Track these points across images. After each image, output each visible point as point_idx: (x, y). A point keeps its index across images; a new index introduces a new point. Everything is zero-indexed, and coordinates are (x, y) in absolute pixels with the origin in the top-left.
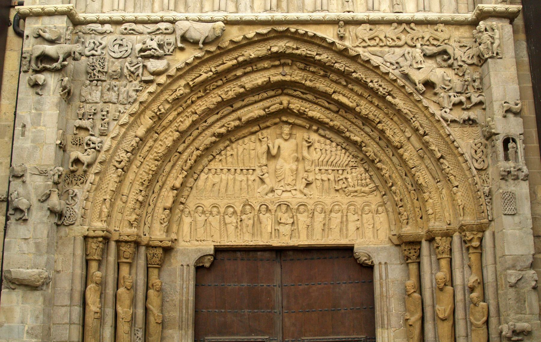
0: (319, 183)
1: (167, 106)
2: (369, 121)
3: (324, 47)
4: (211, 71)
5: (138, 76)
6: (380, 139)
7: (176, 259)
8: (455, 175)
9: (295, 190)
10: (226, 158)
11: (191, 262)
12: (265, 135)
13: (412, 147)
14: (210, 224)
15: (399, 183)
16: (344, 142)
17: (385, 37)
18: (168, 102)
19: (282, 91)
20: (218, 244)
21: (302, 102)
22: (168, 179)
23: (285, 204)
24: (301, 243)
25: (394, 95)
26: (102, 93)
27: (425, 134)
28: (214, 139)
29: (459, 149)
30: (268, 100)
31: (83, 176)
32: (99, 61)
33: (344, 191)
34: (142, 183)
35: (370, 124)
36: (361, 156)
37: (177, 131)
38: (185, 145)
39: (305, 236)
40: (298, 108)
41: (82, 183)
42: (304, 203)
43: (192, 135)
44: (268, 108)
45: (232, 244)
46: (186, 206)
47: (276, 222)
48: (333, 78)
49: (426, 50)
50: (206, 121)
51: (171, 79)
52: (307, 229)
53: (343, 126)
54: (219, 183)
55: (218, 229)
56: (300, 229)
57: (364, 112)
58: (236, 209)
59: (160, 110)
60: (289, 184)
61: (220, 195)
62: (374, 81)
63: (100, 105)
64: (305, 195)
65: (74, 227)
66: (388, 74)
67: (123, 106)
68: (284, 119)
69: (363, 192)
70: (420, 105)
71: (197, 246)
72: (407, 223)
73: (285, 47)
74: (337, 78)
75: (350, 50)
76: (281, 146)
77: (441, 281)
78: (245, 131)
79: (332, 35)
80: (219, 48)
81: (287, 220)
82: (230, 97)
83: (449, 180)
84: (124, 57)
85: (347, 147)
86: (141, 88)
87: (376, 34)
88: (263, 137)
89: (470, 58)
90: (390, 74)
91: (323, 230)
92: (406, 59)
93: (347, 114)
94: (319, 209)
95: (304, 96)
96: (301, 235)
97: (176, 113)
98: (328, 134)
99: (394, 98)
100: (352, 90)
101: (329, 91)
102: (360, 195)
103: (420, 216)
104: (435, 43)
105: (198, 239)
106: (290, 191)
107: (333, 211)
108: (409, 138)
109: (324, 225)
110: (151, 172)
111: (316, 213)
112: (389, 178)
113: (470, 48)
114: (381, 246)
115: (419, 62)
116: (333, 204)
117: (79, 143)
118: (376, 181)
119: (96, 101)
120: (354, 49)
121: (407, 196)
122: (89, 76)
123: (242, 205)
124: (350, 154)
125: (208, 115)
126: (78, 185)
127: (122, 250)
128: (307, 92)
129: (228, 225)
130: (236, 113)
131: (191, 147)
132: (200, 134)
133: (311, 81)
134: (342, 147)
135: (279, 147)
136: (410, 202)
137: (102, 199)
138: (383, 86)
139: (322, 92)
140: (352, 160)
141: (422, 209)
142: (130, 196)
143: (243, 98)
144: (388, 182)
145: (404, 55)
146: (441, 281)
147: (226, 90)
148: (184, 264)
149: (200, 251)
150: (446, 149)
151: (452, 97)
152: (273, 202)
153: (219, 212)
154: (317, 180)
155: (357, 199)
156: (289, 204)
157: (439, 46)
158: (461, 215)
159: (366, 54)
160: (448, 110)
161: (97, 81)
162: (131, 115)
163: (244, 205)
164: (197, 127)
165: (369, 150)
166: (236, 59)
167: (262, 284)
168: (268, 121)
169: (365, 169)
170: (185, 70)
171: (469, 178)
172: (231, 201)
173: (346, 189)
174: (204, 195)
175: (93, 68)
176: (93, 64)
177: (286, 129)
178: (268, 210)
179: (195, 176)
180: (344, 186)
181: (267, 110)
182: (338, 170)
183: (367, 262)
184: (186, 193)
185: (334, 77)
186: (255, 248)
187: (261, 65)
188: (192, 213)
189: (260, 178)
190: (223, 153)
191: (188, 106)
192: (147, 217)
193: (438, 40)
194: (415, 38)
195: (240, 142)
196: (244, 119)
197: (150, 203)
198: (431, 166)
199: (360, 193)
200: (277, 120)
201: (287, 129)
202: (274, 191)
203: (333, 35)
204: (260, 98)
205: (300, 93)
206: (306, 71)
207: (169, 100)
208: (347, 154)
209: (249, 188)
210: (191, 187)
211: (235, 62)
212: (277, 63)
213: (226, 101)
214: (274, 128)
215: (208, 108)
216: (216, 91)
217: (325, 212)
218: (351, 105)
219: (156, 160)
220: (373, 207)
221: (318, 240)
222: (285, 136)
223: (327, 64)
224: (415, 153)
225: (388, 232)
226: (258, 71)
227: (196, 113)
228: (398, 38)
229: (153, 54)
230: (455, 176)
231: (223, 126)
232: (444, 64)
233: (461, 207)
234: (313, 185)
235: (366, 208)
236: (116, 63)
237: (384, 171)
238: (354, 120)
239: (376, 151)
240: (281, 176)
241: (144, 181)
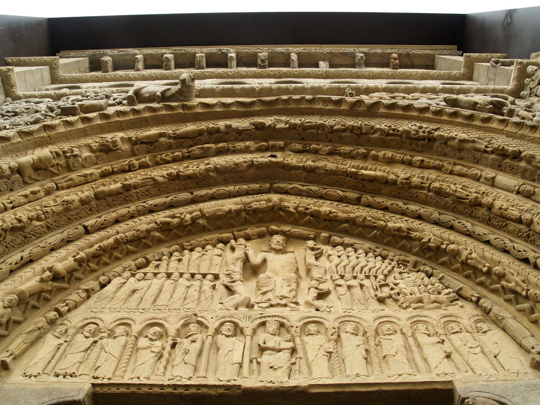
0: (342, 290)
1: (86, 154)
2: (414, 191)
6: (440, 214)
9: (297, 303)
10: (168, 265)
13: (504, 192)
16: (377, 248)
18: (92, 150)
19: (271, 184)
21: (302, 198)
22: (46, 258)
30: (250, 197)
33: (396, 301)
36: (412, 258)
40: (295, 205)
42: (315, 319)
44: (249, 203)
45: (138, 382)
46: (65, 322)
47: (256, 349)
48: (346, 149)
51: (104, 122)
52: (329, 360)
53: (372, 217)
54: (145, 289)
56: (310, 359)
57: (402, 176)
58: (166, 325)
59: (72, 151)
60: (283, 297)
64: (317, 310)
68: (274, 227)
74: (352, 149)
80: (184, 107)
81: (280, 344)
82: (191, 172)
91: (366, 359)
93: (375, 199)
94: (349, 327)
95: (305, 188)
96: (314, 368)
98: (347, 240)
100: (376, 158)
101: (342, 167)
105: (59, 372)
106: (285, 305)
107: (380, 333)
110: (15, 221)
111: (343, 335)
116: (378, 321)
123: (182, 322)
125: (152, 197)
129: (140, 351)
130: (198, 205)
133: (313, 161)
134: (374, 254)
135: (265, 261)
143: (210, 188)
144: (480, 266)
147: (185, 165)
154: (338, 288)
155: (425, 313)
156: (284, 321)
162: (21, 134)
163: (186, 325)
164: (128, 205)
165: (425, 234)
168: (247, 229)
169: (426, 273)
172: (161, 316)
174: (108, 306)
177: (278, 239)
178: (238, 330)
182: (376, 277)
184: (74, 297)
185: (347, 149)
187: (241, 145)
188: (71, 331)
195: (198, 249)
199: (429, 303)
200: (263, 229)
201: (278, 238)
202: (253, 306)
206: (305, 154)
208: (387, 261)
209: (203, 295)
210: (87, 291)
213: (183, 176)
214: (257, 243)
215: (153, 179)
216: (170, 165)
217: (365, 333)
221: (357, 375)
222: (276, 246)
223: (335, 128)
225: (522, 358)
226: (235, 152)
234: (332, 297)
237: (465, 253)
240: (267, 286)
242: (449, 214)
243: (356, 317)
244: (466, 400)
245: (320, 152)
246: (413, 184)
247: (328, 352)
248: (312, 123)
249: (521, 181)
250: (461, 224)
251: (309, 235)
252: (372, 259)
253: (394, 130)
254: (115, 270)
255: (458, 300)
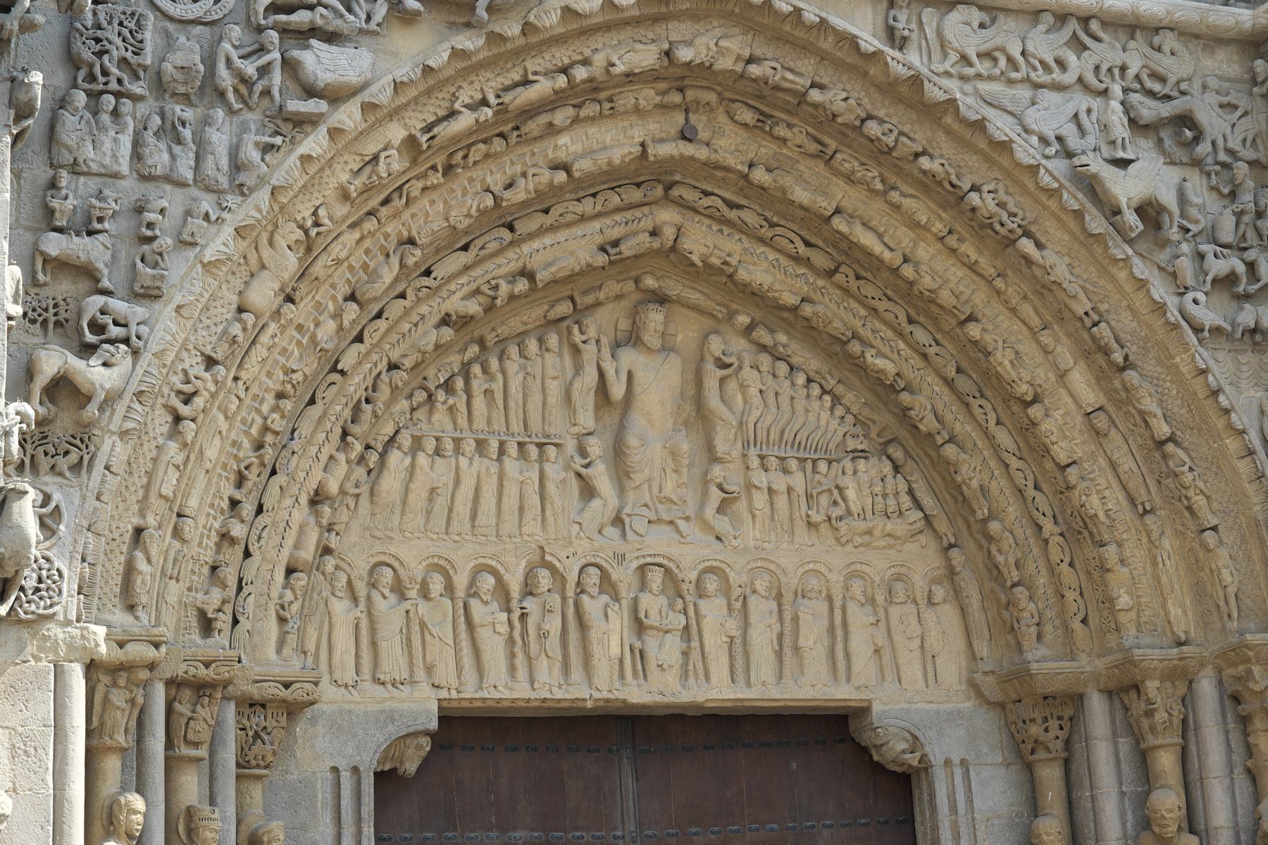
0: (760, 499)
1: (341, 210)
2: (934, 309)
3: (839, 64)
4: (484, 102)
5: (267, 93)
6: (959, 370)
7: (313, 746)
8: (1207, 493)
11: (366, 758)
12: (592, 332)
14: (423, 625)
15: (1010, 509)
17: (1023, 53)
20: (454, 695)
21: (721, 231)
23: (660, 565)
24: (714, 694)
25: (1038, 235)
26: (137, 143)
27: (1127, 365)
28: (447, 333)
29: (1233, 415)
31: (78, 442)
32: (121, 24)
34: (240, 472)
35: (935, 320)
37: (352, 297)
38: (362, 348)
39: (726, 673)
41: (76, 467)
43: (385, 316)
44: (616, 243)
45: (497, 696)
49: (1139, 106)
50: (427, 273)
55: (451, 642)
57: (927, 282)
59: (317, 224)
61: (454, 528)
62: (985, 188)
63: (130, 187)
65: (55, 631)
66: (1034, 169)
67: (216, 196)
68: (650, 282)
69: (889, 535)
70: (1122, 275)
71: (383, 701)
72: (1039, 637)
73: (715, 49)
75: (926, 82)
76: (639, 375)
77: (1171, 815)
78: (534, 315)
79: (870, 27)
80: (528, 28)
83: (1189, 508)
84: (209, 19)
85: (840, 389)
86: (278, 140)
87: (998, 41)
88: (584, 338)
89: (1248, 144)
90: (1042, 171)
92: (1080, 127)
94: (761, 585)
95: (732, 215)
97: (357, 235)
99: (1039, 245)
102: (882, 543)
103: (1081, 616)
104: (1157, 87)
108: (1062, 375)
109: (781, 636)
112: (979, 494)
113: (1246, 113)
114: (946, 706)
115: (1119, 141)
116: (801, 570)
117: (53, 319)
118: (927, 501)
119: (116, 168)
120: (936, 79)
121: (1036, 551)
122: (82, 74)
124: (848, 411)
126: (61, 474)
127: (181, 714)
128: (743, 202)
131: (375, 357)
132: (407, 312)
134: (822, 387)
135: (630, 375)
136: (1044, 571)
137: (130, 527)
138: (1012, 208)
139: (801, 207)
140: (853, 430)
141: (1085, 594)
142: (202, 520)
145: (1076, 115)
146: (1171, 815)
148: (343, 764)
149: (393, 721)
150: (1184, 411)
151: (1210, 257)
152: (623, 556)
153: (449, 588)
154: (753, 491)
157: (1168, 98)
158: (1229, 616)
159: (969, 100)
160: (1201, 297)
161: (118, 95)
166: (564, 70)
167: (578, 834)
170: (413, 92)
171: (1254, 504)
173: (843, 523)
175: (98, 47)
176: (99, 33)
179: (373, 458)
180: (836, 512)
181: (611, 251)
182: (814, 461)
183: (907, 756)
185: (846, 161)
186: (571, 708)
187: (626, 100)
189: (579, 475)
190: (459, 383)
191: (396, 215)
192: (243, 595)
193: (1162, 80)
194: (1104, 68)
196: (543, 276)
197: (251, 548)
198: (1127, 464)
203: (874, 28)
204: (598, 207)
205: (720, 201)
207: (352, 188)
208: (839, 411)
209: (548, 506)
211: (562, 81)
212: (676, 98)
218: (887, 255)
219: (280, 396)
220: (919, 582)
224: (1079, 419)
227: (411, 242)
228: (1061, 64)
229: (319, 22)
230: (1208, 498)
231: (477, 291)
232: (1180, 154)
233: (1231, 590)
234: (742, 506)
235: (899, 587)
236: (182, 39)
238: (882, 306)
239: (940, 407)
241: (247, 468)
242: (974, 376)
243: (772, 562)
244: (879, 730)
245: (789, 144)
246: (939, 301)
247: (729, 637)
248: (797, 84)
249: (1102, 400)
250: (983, 411)
251: (715, 310)
252: (816, 404)
253: (953, 185)
254: (383, 432)
255: (921, 532)
